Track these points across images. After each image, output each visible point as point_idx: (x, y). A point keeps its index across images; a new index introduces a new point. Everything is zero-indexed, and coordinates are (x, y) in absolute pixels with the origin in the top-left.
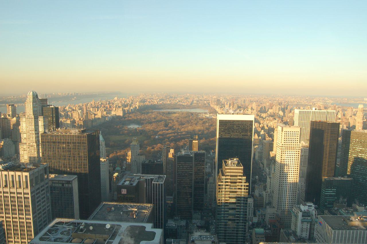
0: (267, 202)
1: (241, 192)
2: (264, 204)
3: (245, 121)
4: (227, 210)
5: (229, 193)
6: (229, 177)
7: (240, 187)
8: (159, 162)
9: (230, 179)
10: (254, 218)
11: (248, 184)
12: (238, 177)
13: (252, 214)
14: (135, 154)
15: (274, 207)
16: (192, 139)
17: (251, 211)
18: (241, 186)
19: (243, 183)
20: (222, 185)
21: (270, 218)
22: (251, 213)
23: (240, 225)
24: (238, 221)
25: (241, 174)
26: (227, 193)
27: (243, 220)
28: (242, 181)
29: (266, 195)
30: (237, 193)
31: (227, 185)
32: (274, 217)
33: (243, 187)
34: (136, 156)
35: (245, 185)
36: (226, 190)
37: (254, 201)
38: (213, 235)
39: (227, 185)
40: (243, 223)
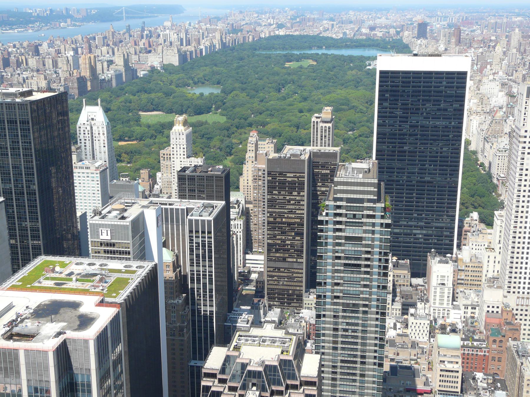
0: (490, 275)
1: (373, 240)
2: (483, 280)
3: (448, 73)
4: (339, 281)
5: (343, 241)
6: (344, 203)
7: (371, 228)
8: (219, 170)
9: (347, 208)
10: (452, 312)
11: (389, 221)
12: (366, 205)
13: (448, 300)
14: (182, 155)
15: (499, 287)
16: (319, 120)
17: (446, 295)
18: (374, 225)
19: (378, 218)
20: (327, 221)
21: (488, 311)
22: (446, 298)
23: (371, 319)
24: (367, 309)
25: (372, 197)
26: (340, 241)
27: (378, 307)
28: (374, 214)
29: (489, 257)
30: (364, 242)
31: (340, 223)
32: (498, 310)
33: (377, 228)
34: (182, 160)
35: (382, 224)
36: (338, 234)
37: (457, 271)
38: (289, 337)
39: (340, 223)
40: (377, 313)
